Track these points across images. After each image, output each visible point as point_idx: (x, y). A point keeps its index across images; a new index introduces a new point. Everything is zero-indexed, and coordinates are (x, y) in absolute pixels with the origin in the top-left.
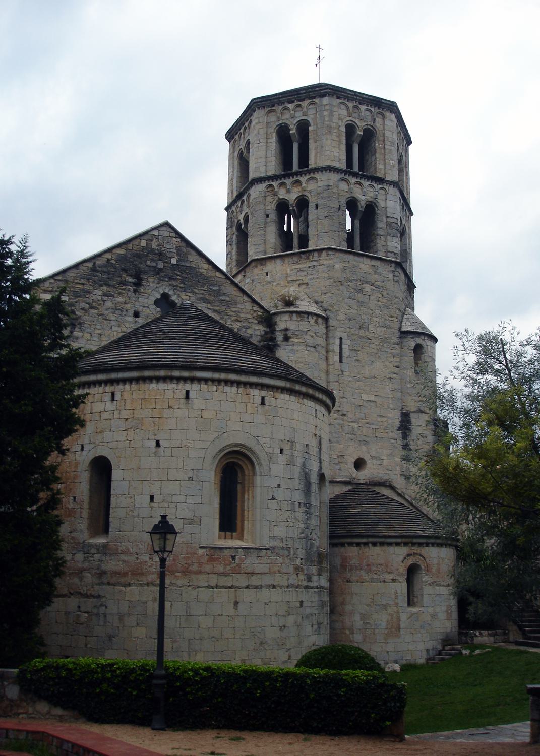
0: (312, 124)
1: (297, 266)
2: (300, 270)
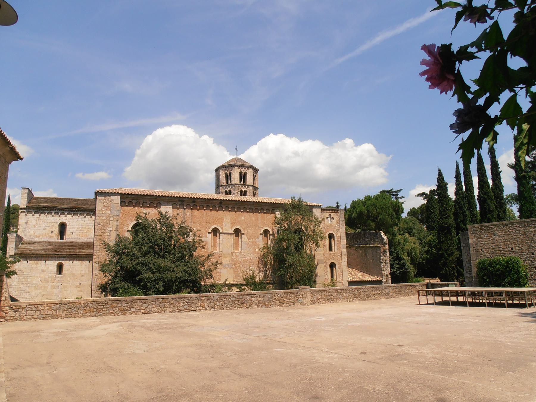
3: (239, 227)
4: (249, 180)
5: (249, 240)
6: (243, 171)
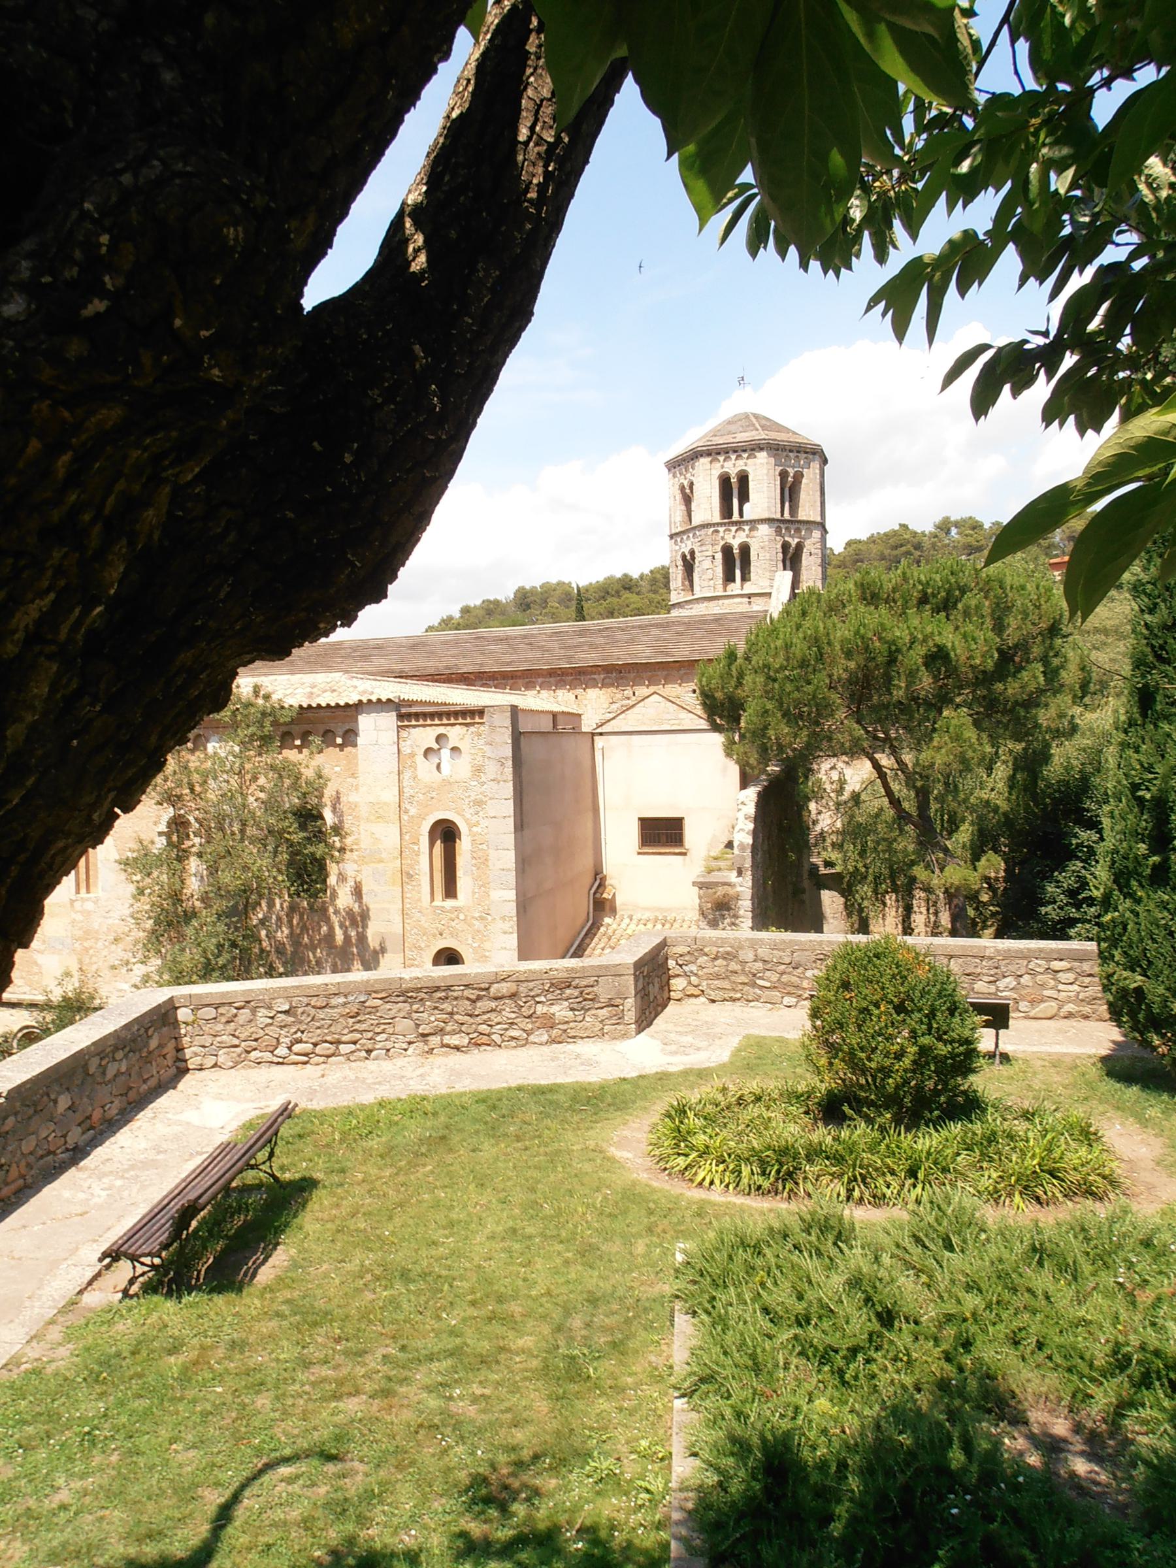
4: (763, 500)
6: (732, 467)
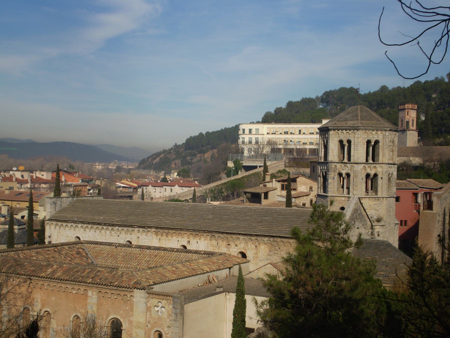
0: (381, 142)
1: (375, 203)
2: (375, 204)
3: (48, 310)
5: (58, 327)
